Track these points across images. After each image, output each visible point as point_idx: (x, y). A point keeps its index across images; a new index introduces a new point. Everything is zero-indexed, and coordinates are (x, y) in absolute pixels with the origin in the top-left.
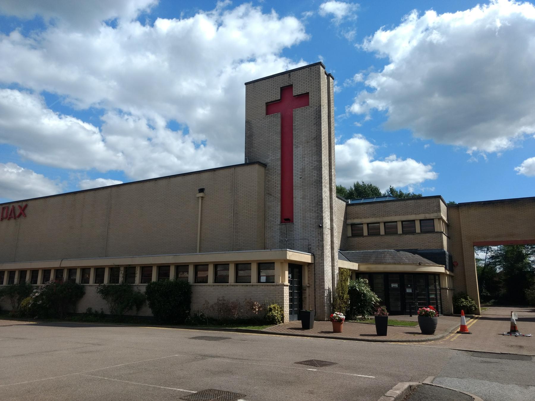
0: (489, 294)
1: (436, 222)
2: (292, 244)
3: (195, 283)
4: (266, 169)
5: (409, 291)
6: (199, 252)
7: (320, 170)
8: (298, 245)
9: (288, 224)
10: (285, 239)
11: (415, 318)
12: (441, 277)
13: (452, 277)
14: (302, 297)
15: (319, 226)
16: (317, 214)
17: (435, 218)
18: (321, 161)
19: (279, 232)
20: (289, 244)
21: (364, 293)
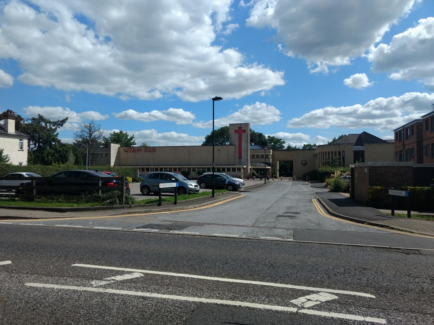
5: (262, 173)
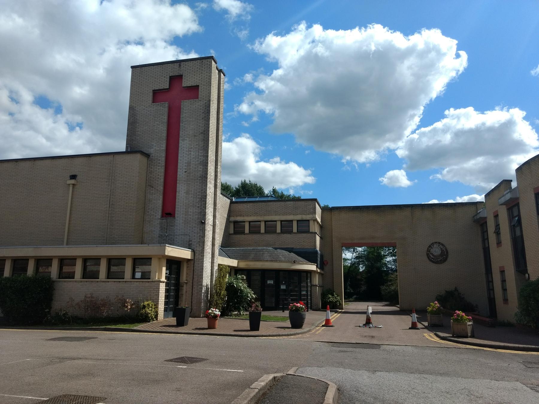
0: (352, 291)
1: (311, 223)
2: (172, 240)
3: (59, 278)
4: (149, 159)
5: (283, 287)
6: (67, 245)
7: (206, 165)
8: (178, 241)
9: (170, 219)
10: (165, 234)
11: (287, 313)
12: (313, 274)
13: (322, 274)
14: (179, 293)
15: (202, 222)
16: (200, 210)
17: (310, 219)
18: (207, 156)
19: (159, 226)
20: (169, 239)
21: (241, 290)
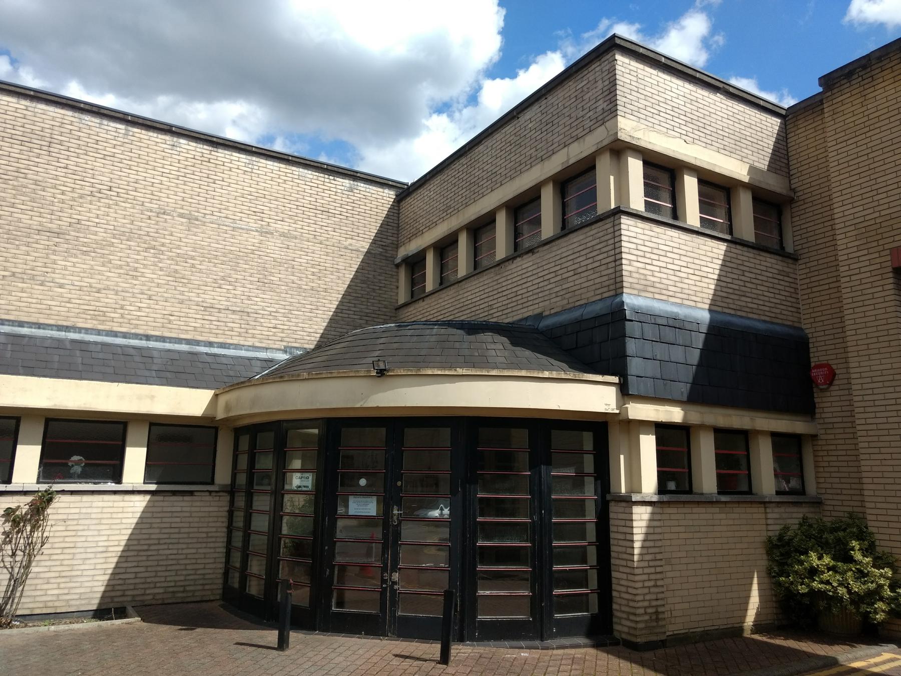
12: (615, 438)
